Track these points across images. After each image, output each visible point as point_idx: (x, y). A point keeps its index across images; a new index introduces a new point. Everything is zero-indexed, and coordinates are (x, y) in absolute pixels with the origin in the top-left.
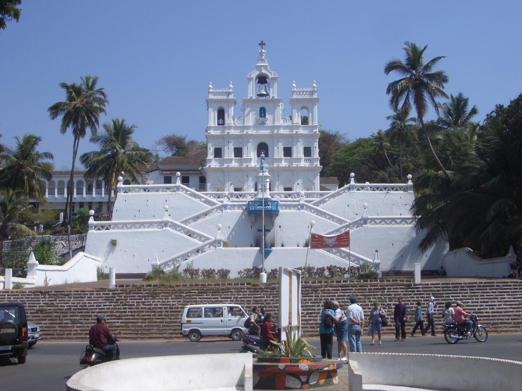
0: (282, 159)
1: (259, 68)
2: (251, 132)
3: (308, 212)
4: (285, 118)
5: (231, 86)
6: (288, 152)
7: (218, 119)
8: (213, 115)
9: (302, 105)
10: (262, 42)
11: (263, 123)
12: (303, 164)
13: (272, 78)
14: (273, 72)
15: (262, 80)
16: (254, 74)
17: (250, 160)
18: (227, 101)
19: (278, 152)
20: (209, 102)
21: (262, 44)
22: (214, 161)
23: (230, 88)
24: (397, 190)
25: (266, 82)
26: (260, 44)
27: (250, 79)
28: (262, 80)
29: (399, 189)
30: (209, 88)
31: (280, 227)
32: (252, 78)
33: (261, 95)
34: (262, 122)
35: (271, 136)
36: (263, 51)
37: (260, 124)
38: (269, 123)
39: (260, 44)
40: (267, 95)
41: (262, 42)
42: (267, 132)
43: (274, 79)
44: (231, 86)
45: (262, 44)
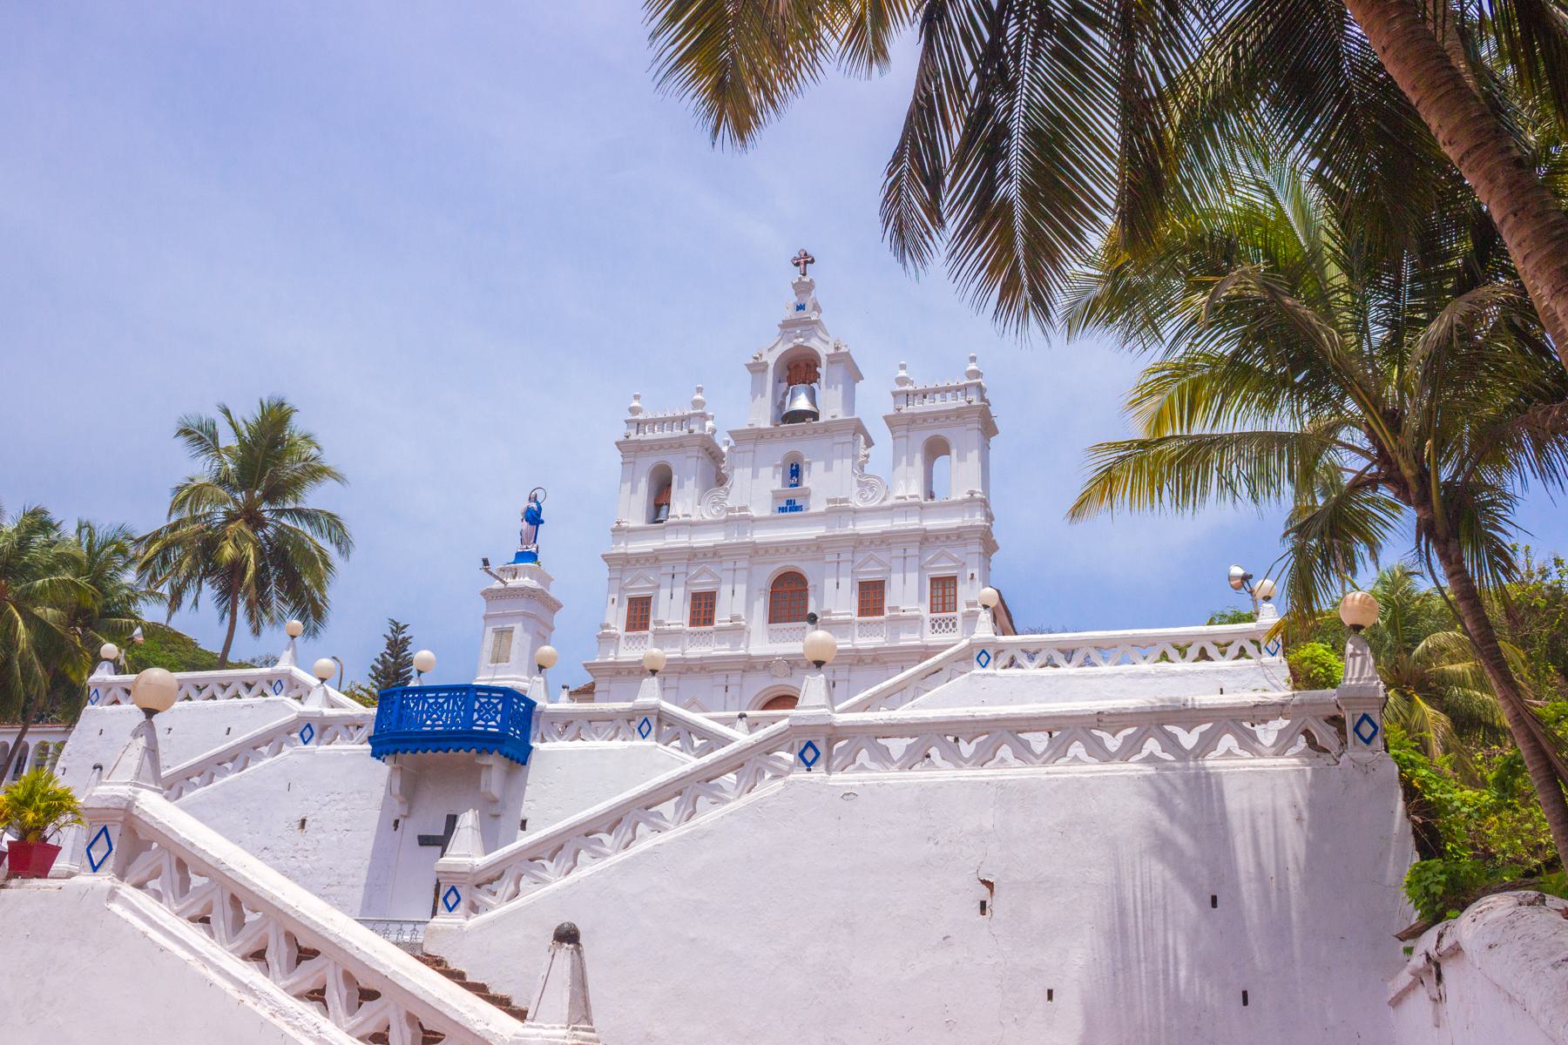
2: (761, 536)
4: (867, 484)
6: (871, 597)
17: (737, 630)
19: (835, 596)
24: (1203, 655)
32: (766, 365)
34: (789, 502)
35: (818, 545)
37: (782, 510)
38: (817, 505)
45: (804, 261)
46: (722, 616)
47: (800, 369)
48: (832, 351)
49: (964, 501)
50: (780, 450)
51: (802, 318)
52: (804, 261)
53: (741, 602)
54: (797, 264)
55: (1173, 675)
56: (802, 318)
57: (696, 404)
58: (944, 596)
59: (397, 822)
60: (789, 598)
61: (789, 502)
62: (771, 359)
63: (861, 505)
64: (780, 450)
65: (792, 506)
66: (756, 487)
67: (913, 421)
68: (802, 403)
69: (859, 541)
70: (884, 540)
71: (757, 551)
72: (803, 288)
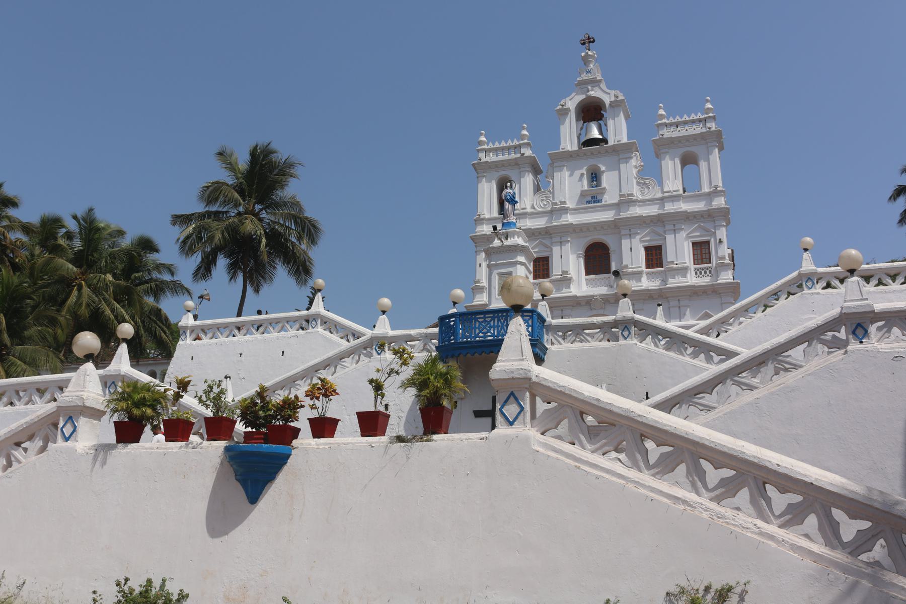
0: (640, 273)
1: (583, 85)
4: (644, 184)
5: (525, 132)
6: (654, 256)
8: (487, 193)
11: (595, 199)
12: (691, 279)
13: (611, 103)
14: (613, 92)
15: (591, 112)
16: (572, 102)
17: (565, 280)
18: (515, 163)
19: (631, 254)
20: (481, 169)
21: (588, 41)
23: (523, 137)
27: (564, 112)
28: (591, 112)
30: (480, 143)
32: (568, 109)
34: (593, 197)
36: (590, 53)
40: (604, 141)
42: (607, 216)
43: (615, 104)
44: (525, 132)
46: (556, 271)
48: (613, 99)
53: (569, 261)
54: (583, 44)
58: (701, 254)
60: (598, 259)
61: (593, 197)
63: (641, 198)
68: (595, 134)
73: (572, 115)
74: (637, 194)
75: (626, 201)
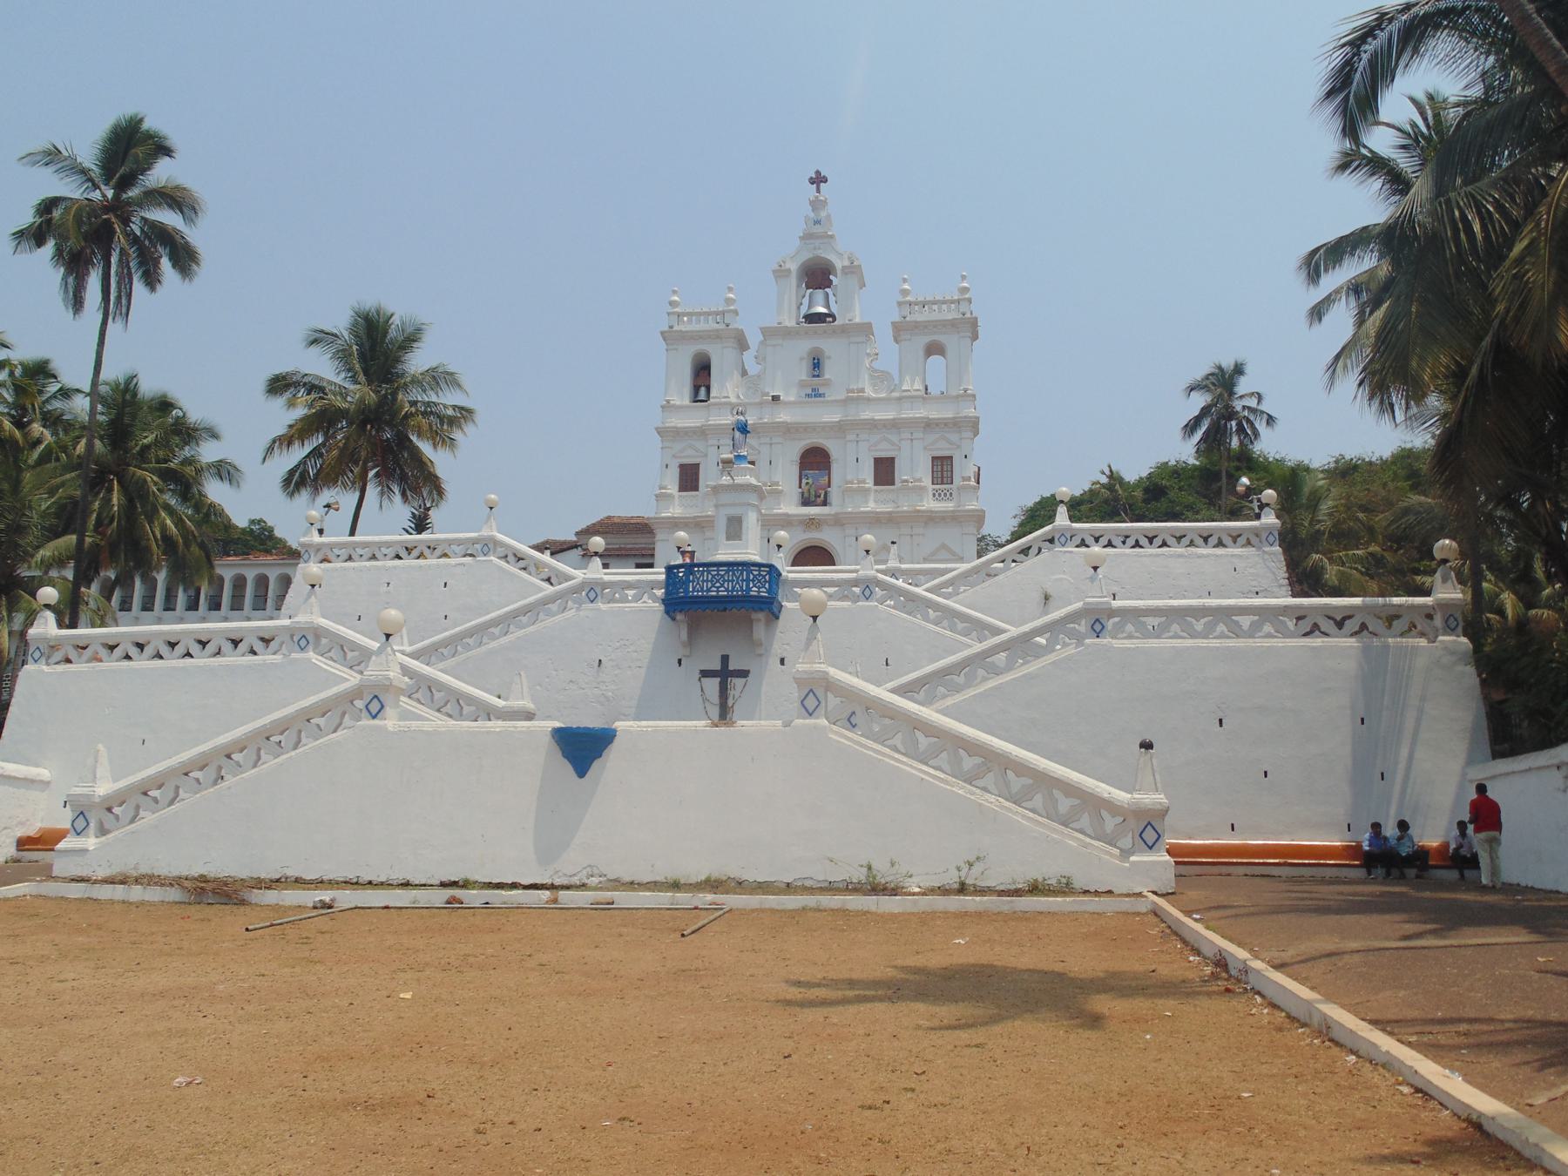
0: (868, 490)
2: (784, 416)
3: (887, 608)
6: (885, 471)
7: (696, 389)
9: (927, 339)
10: (818, 172)
11: (816, 394)
12: (929, 504)
18: (715, 336)
22: (677, 501)
24: (1220, 544)
25: (829, 284)
26: (812, 181)
29: (1227, 540)
31: (782, 661)
32: (789, 271)
33: (813, 318)
35: (840, 429)
39: (812, 181)
41: (818, 172)
45: (818, 180)
47: (817, 276)
48: (847, 263)
49: (958, 397)
50: (804, 346)
51: (816, 231)
52: (818, 180)
55: (1200, 556)
56: (816, 231)
57: (729, 301)
59: (680, 661)
62: (793, 266)
64: (804, 346)
65: (816, 394)
66: (786, 377)
67: (917, 327)
69: (873, 425)
70: (895, 425)
71: (788, 430)
72: (817, 205)
73: (793, 280)
74: (870, 392)
75: (855, 399)
